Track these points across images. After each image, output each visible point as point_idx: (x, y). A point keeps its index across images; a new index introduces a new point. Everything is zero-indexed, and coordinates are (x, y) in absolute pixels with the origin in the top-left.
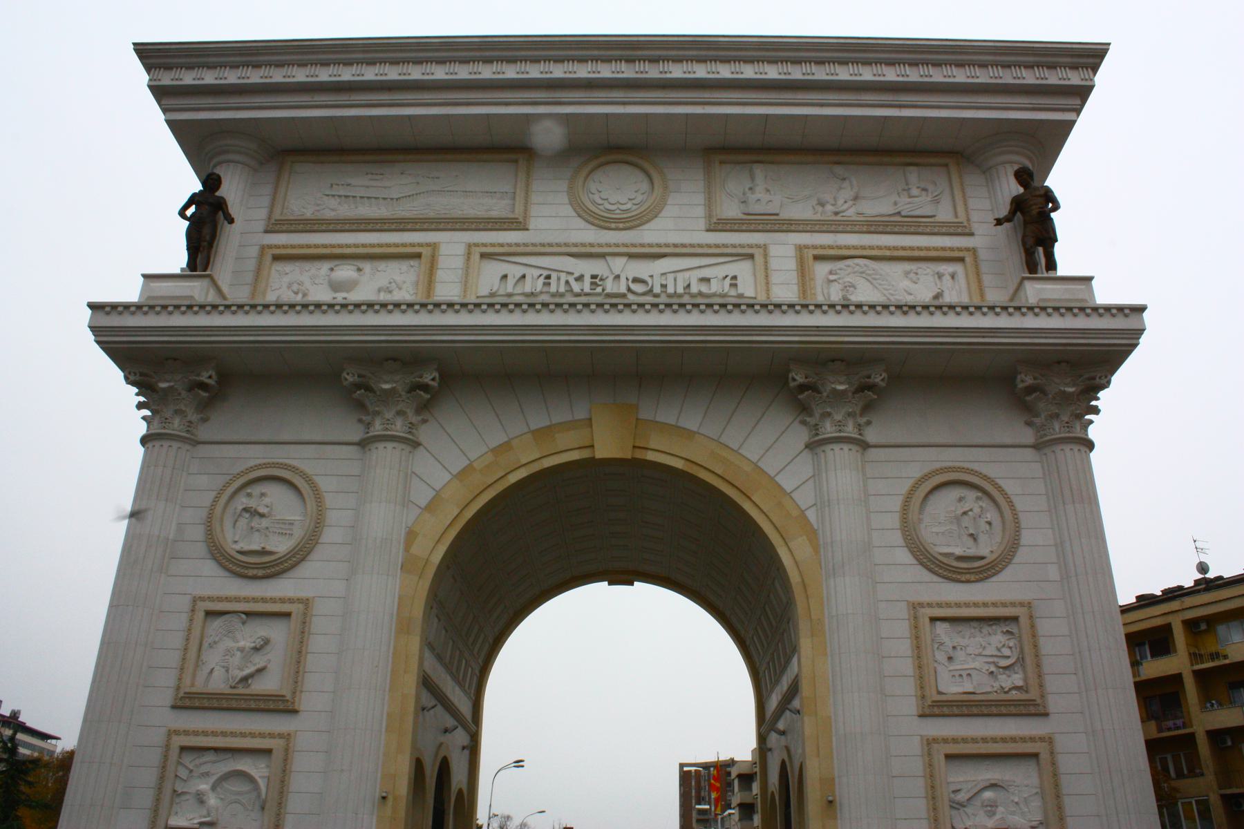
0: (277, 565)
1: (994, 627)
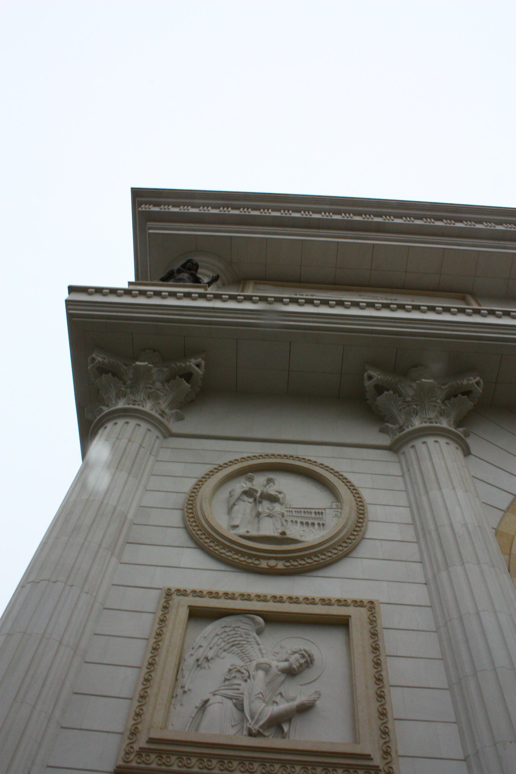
0: (309, 556)
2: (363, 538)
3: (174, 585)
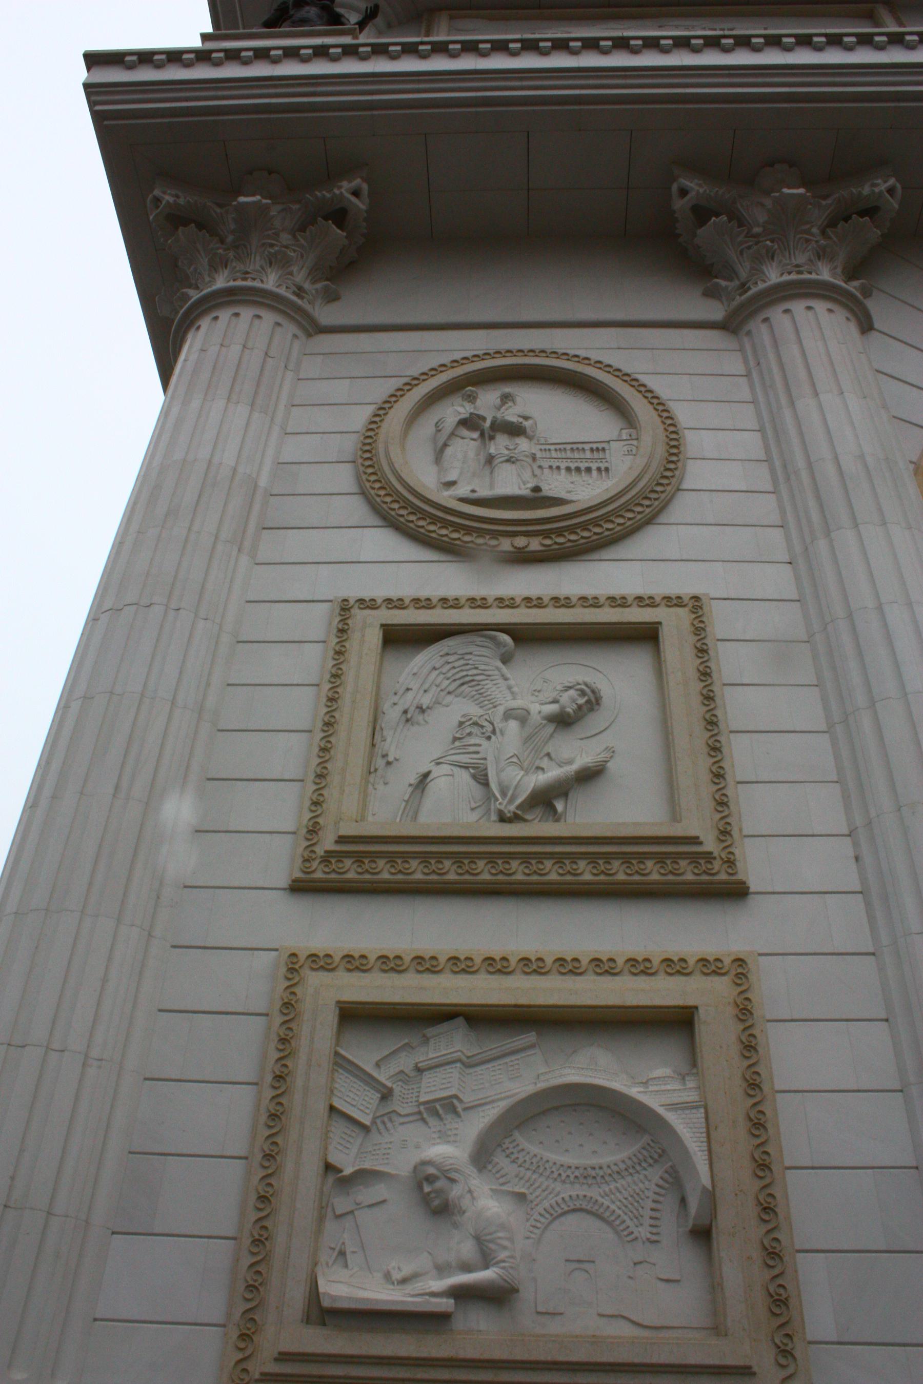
0: (584, 526)
2: (678, 490)
3: (353, 592)
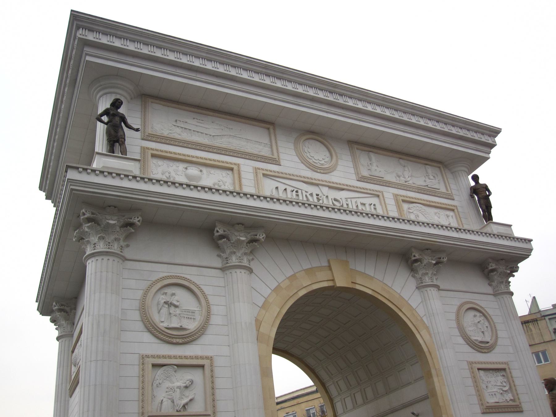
1: (498, 373)
